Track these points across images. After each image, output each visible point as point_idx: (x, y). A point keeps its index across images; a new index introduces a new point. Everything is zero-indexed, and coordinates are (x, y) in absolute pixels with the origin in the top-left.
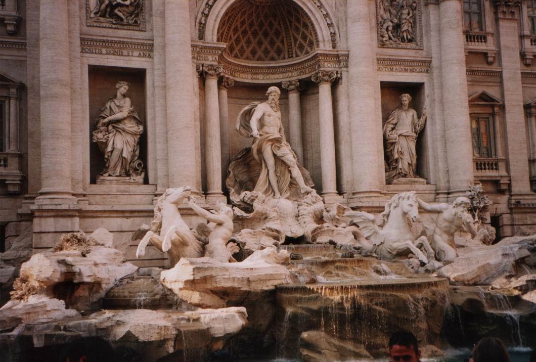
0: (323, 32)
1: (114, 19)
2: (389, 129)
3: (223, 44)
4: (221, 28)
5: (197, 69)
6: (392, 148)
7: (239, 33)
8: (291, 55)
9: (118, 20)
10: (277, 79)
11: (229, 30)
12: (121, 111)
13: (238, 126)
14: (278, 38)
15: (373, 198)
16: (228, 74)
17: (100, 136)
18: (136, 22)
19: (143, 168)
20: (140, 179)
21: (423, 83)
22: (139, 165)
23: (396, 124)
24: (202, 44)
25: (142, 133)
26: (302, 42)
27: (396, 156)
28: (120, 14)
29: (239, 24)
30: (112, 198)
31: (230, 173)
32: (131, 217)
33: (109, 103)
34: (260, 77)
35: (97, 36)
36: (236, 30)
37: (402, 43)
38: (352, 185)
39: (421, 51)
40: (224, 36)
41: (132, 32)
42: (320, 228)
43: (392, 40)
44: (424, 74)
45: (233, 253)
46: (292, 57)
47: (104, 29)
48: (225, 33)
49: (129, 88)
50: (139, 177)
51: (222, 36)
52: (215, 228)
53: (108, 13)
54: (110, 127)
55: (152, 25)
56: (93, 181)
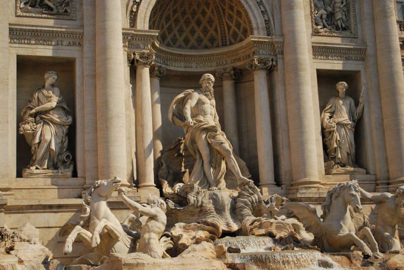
0: (257, 19)
1: (44, 9)
3: (155, 32)
4: (154, 16)
6: (330, 137)
7: (172, 19)
8: (224, 44)
9: (48, 9)
10: (211, 66)
11: (161, 19)
12: (49, 102)
13: (170, 115)
14: (211, 26)
15: (313, 189)
16: (161, 63)
17: (28, 127)
19: (71, 161)
20: (69, 172)
21: (359, 71)
22: (68, 157)
23: (334, 112)
24: (133, 32)
25: (70, 123)
26: (237, 30)
30: (39, 192)
31: (162, 164)
32: (58, 212)
33: (37, 94)
34: (194, 65)
35: (26, 26)
36: (168, 19)
37: (336, 31)
38: (291, 174)
39: (355, 40)
40: (156, 25)
41: (61, 21)
42: (258, 221)
43: (326, 28)
44: (360, 62)
45: (166, 249)
46: (226, 45)
47: (34, 19)
48: (157, 22)
49: (58, 77)
50: (67, 170)
51: (154, 23)
52: (148, 221)
53: (38, 3)
54: (38, 118)
55: (82, 14)
56: (19, 175)
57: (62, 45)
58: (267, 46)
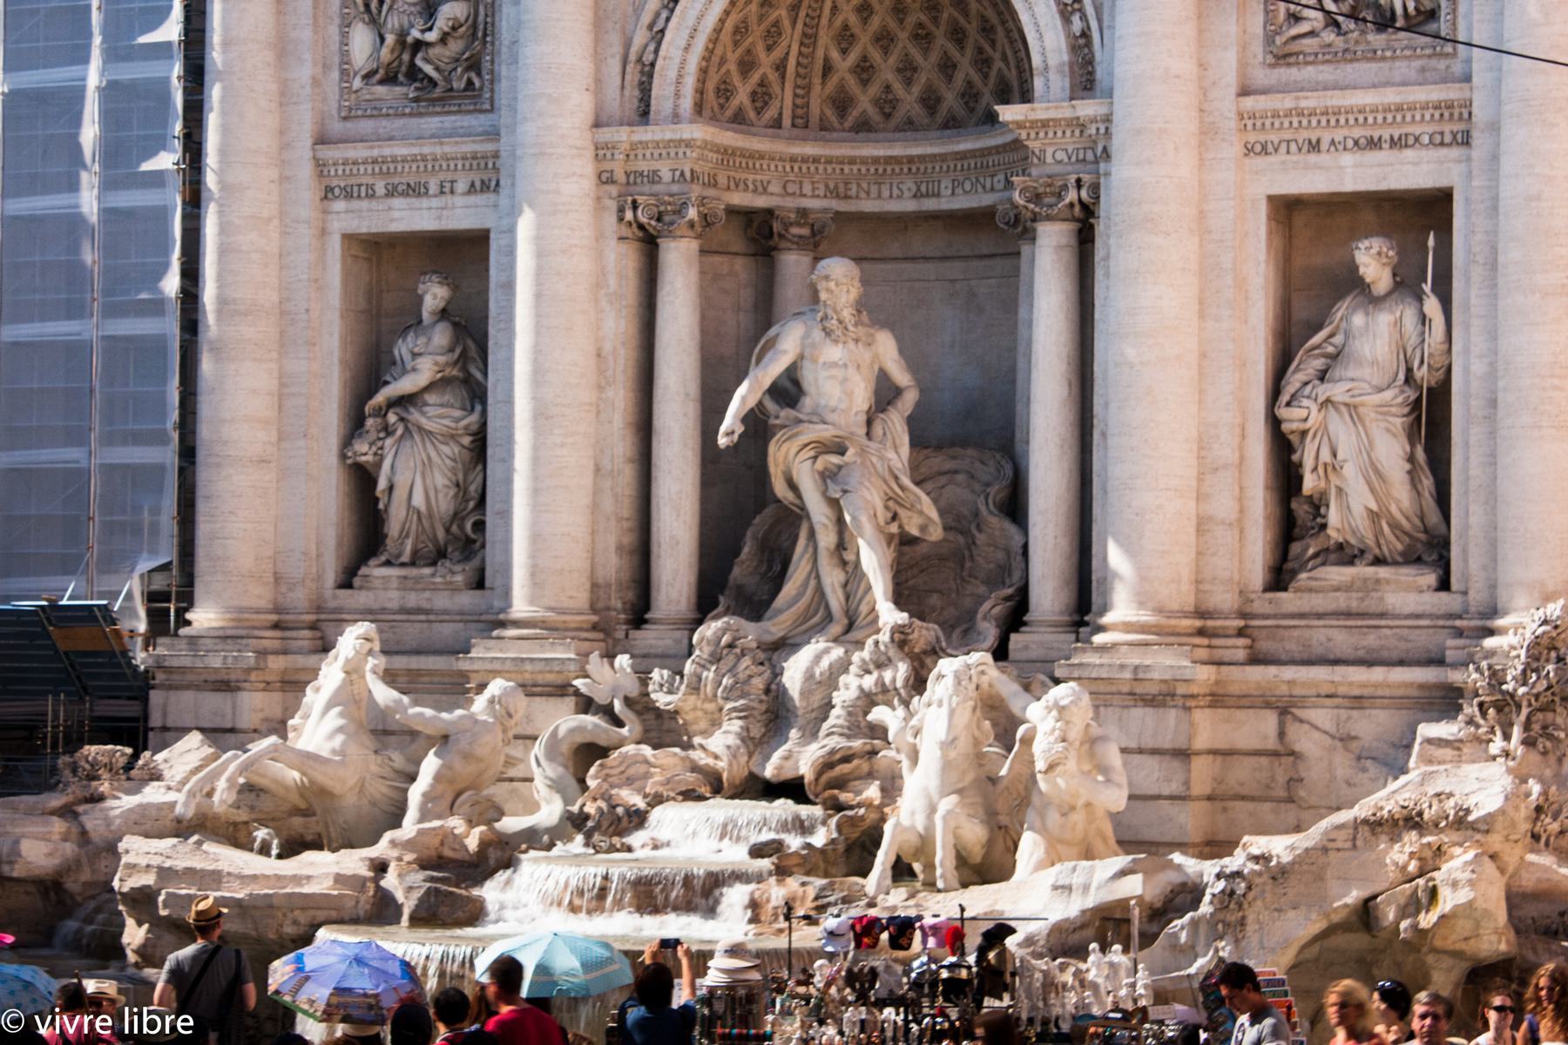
2: (1301, 377)
4: (769, 49)
5: (621, 219)
7: (864, 41)
12: (414, 370)
16: (813, 196)
17: (363, 450)
18: (470, 83)
25: (475, 427)
27: (1309, 484)
28: (428, 69)
29: (848, 15)
34: (946, 184)
36: (845, 38)
41: (453, 118)
44: (1455, 152)
48: (792, 62)
49: (455, 288)
50: (458, 568)
51: (781, 67)
57: (452, 192)
58: (1068, 133)
